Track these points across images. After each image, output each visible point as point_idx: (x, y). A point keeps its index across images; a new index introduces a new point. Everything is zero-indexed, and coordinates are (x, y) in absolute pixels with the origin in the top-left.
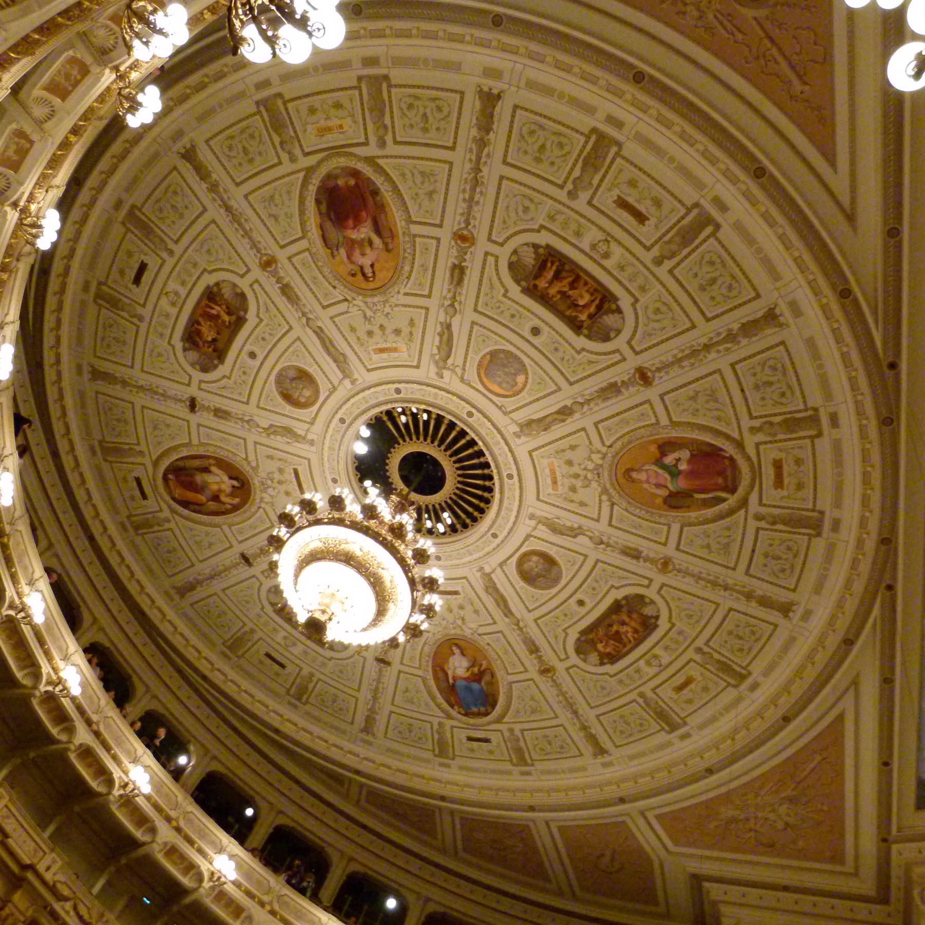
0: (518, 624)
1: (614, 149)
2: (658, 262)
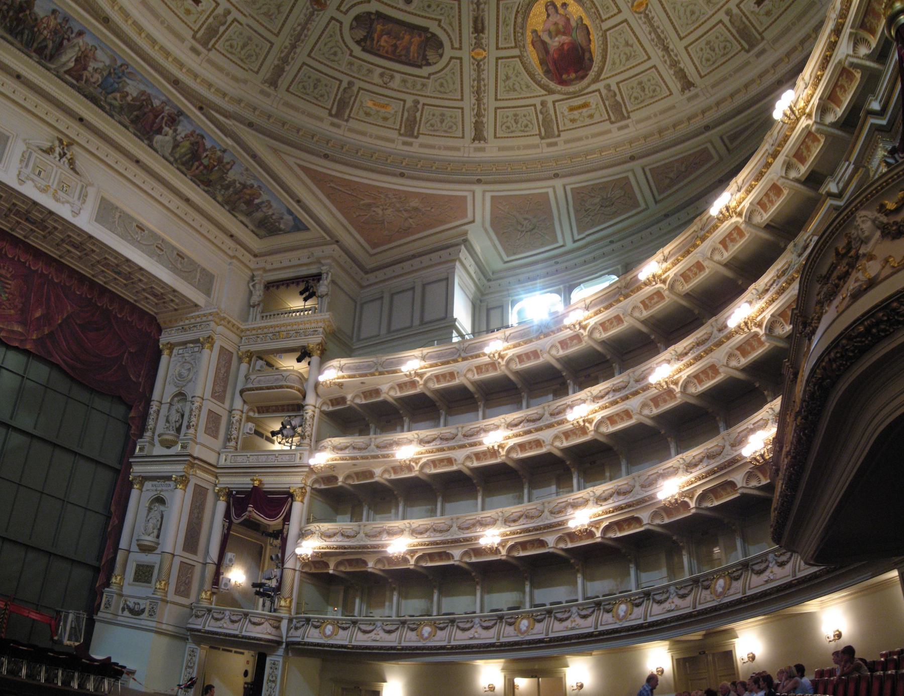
1: (402, 131)
2: (350, 84)
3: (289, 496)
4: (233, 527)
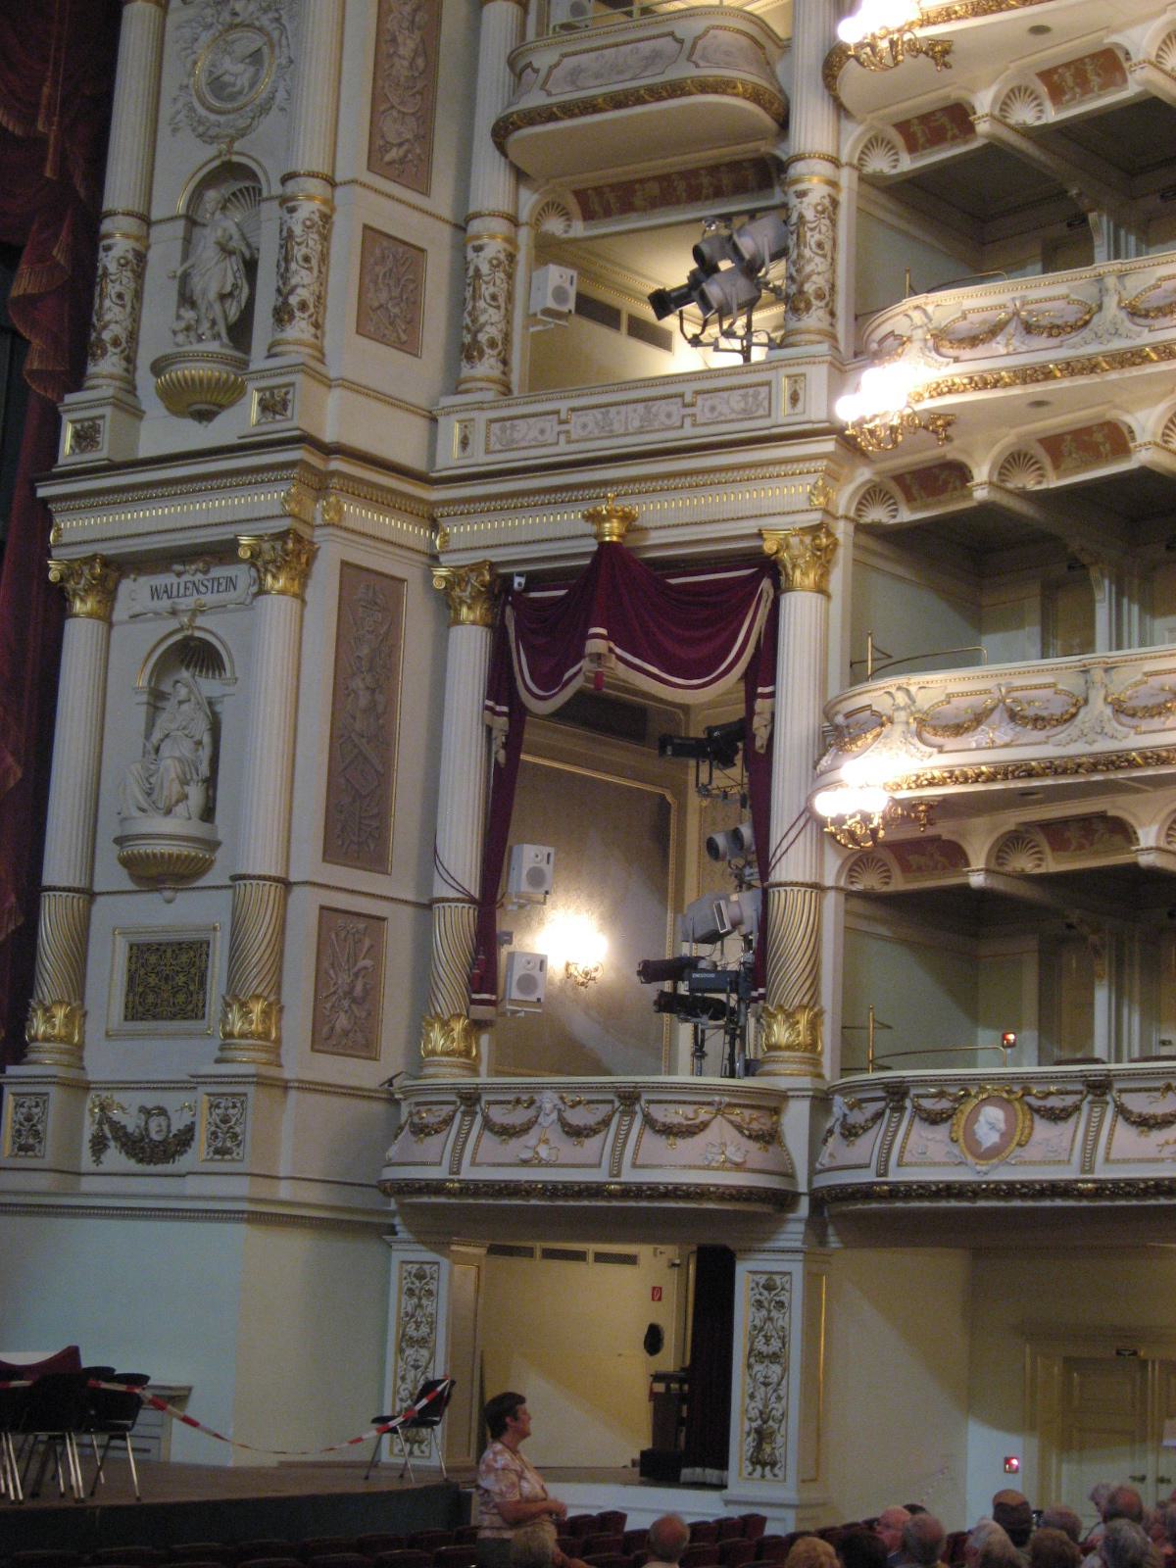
3: (757, 573)
4: (530, 735)
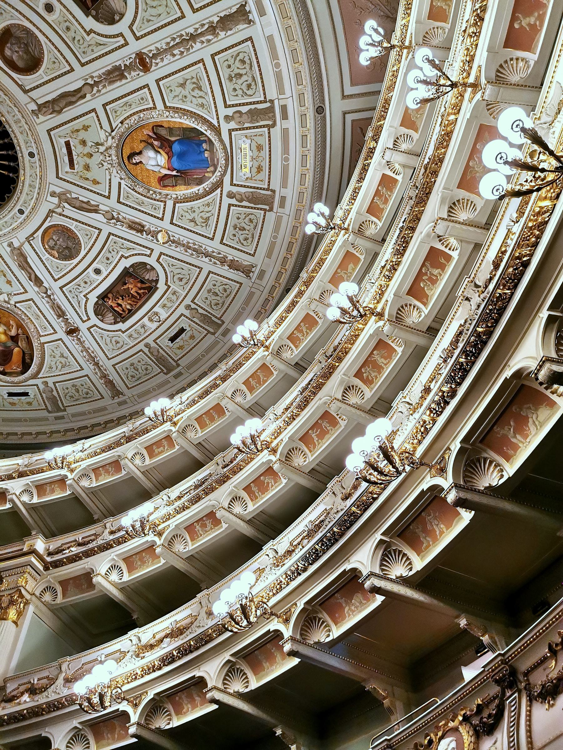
0: (92, 86)
